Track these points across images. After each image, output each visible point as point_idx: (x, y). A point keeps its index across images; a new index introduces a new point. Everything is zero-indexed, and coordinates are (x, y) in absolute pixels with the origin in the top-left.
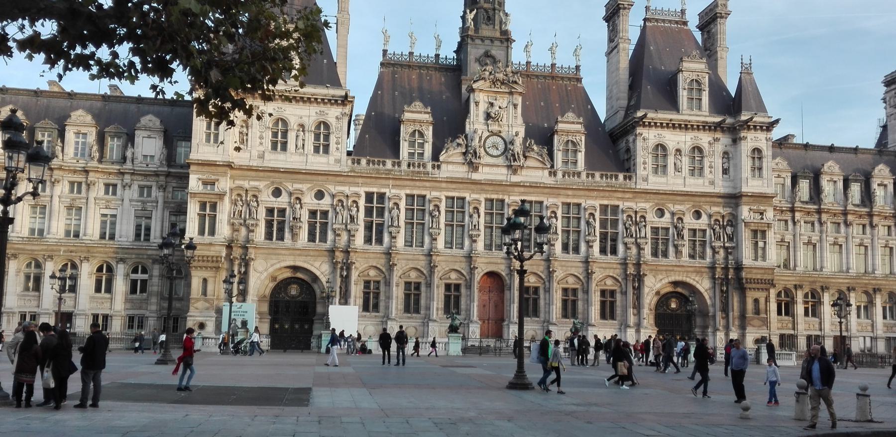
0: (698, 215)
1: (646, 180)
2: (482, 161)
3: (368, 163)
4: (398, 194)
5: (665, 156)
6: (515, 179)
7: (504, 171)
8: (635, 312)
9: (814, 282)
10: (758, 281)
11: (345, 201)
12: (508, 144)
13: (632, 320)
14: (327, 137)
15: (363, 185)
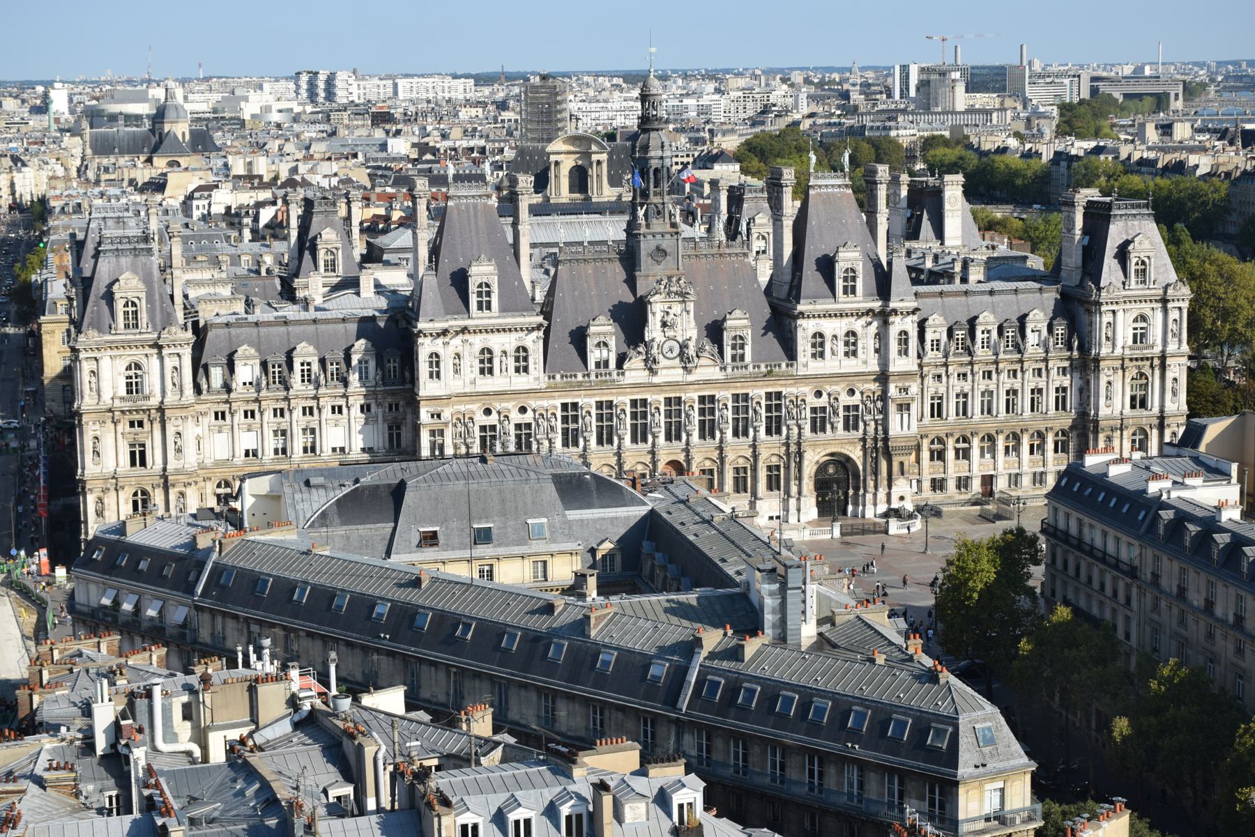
0: (851, 392)
1: (806, 365)
2: (661, 365)
3: (562, 377)
4: (588, 402)
5: (822, 345)
6: (690, 378)
7: (681, 371)
8: (797, 482)
9: (965, 429)
10: (902, 448)
11: (545, 413)
12: (683, 346)
13: (794, 489)
14: (526, 359)
15: (559, 397)
